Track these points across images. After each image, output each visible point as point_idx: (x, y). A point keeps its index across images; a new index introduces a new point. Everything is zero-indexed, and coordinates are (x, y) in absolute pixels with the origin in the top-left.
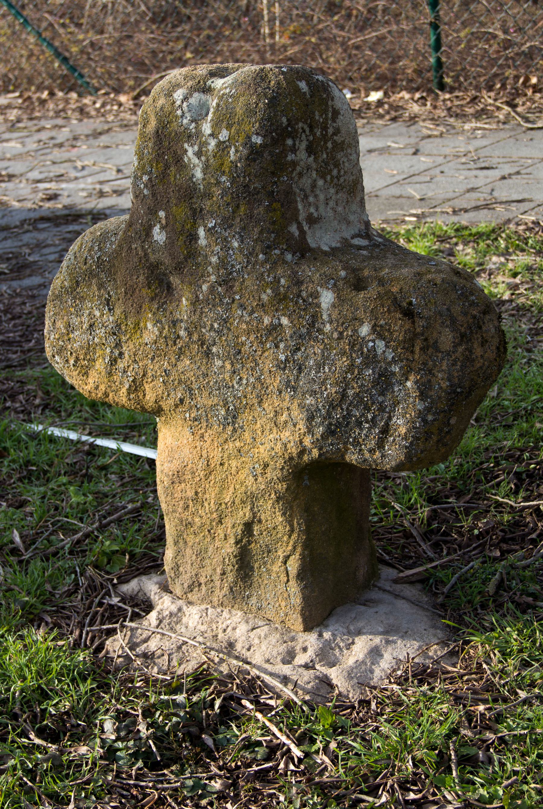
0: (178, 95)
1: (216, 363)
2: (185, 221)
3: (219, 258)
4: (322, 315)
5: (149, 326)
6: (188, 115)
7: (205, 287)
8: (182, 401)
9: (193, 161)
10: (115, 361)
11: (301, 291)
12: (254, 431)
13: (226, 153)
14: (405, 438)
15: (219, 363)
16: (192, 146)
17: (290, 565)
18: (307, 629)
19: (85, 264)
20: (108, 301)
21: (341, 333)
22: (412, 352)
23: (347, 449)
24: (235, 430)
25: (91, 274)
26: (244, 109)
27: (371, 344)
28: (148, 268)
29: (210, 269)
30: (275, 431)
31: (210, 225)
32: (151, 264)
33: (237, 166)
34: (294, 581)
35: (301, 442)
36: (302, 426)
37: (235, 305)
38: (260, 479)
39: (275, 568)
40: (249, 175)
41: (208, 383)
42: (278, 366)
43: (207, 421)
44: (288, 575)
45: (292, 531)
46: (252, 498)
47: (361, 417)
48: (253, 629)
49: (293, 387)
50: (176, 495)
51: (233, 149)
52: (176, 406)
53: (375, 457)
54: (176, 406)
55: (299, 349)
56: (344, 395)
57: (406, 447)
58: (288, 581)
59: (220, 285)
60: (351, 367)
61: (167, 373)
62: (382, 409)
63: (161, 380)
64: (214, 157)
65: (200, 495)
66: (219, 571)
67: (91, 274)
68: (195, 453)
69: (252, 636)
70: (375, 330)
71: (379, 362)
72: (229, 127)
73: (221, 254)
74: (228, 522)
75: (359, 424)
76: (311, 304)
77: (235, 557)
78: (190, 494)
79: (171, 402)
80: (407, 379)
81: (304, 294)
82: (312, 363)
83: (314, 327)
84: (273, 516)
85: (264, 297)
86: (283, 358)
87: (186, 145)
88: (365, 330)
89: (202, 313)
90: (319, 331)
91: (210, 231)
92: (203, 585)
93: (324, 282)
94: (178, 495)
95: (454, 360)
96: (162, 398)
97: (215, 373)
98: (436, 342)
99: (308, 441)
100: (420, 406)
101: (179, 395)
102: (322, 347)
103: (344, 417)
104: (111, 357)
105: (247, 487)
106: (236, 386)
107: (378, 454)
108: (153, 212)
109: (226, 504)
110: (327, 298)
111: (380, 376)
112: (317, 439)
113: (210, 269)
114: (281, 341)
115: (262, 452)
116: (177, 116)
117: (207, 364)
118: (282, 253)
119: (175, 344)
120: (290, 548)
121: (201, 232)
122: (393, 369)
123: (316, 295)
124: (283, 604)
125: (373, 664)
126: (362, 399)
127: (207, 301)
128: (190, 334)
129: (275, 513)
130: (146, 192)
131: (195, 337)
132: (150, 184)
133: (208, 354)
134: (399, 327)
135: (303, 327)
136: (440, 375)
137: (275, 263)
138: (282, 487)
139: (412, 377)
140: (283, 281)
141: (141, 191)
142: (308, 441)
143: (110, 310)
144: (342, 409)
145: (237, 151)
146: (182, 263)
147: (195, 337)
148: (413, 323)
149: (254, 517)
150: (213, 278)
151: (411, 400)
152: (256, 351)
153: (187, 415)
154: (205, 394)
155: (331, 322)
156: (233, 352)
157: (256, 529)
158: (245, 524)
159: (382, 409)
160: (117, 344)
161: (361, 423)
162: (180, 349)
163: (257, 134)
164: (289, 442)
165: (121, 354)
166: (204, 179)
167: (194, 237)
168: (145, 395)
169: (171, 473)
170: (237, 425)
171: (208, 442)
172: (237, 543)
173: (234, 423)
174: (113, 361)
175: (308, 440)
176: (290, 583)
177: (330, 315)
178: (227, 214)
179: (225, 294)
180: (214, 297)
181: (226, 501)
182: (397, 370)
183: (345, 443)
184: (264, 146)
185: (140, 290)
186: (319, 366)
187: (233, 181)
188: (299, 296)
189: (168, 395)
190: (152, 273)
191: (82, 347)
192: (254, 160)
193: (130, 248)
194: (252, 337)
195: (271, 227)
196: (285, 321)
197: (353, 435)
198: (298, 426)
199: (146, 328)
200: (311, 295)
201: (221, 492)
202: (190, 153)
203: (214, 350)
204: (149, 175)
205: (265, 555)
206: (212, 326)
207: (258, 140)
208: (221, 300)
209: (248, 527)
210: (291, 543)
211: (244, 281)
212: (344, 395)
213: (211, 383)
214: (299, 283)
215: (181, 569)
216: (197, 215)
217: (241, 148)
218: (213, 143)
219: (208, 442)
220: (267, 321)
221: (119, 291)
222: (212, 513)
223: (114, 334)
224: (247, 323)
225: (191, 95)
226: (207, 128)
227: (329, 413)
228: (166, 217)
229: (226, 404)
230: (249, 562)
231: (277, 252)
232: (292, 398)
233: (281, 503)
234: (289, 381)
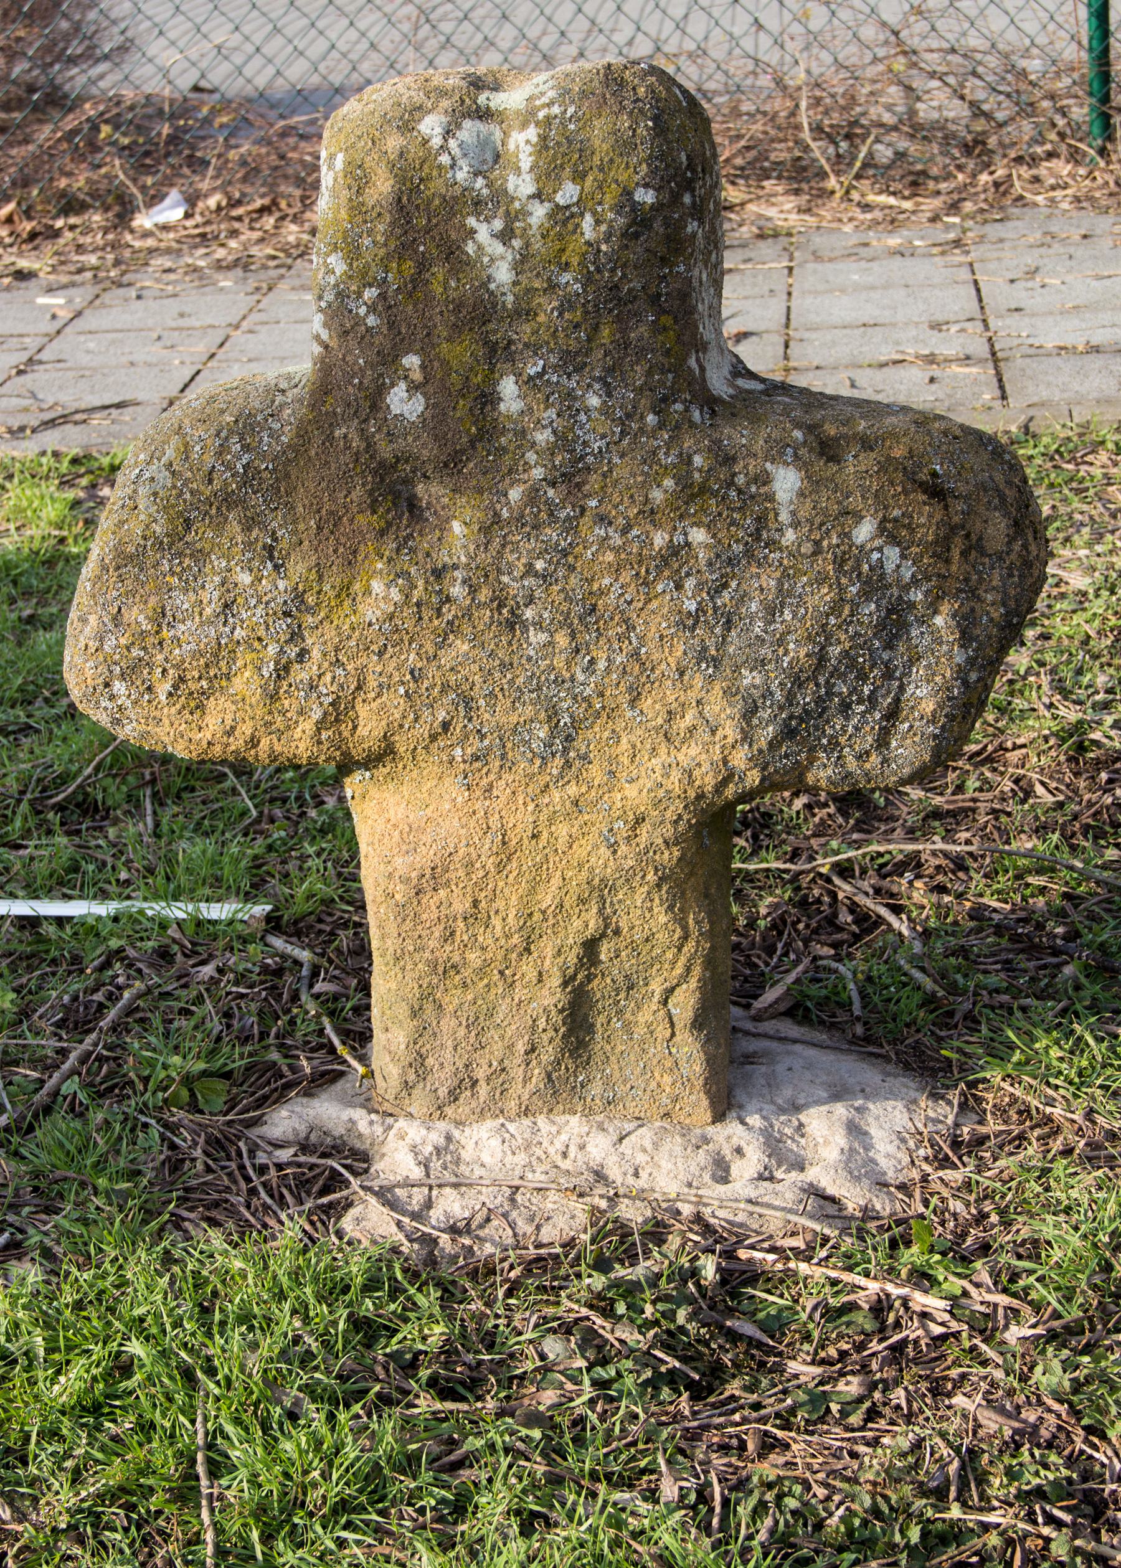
0: (431, 126)
1: (532, 639)
2: (471, 369)
3: (554, 432)
4: (777, 515)
5: (377, 586)
6: (462, 162)
7: (515, 494)
8: (446, 726)
9: (489, 250)
10: (286, 669)
11: (734, 475)
12: (613, 759)
13: (570, 227)
14: (933, 721)
15: (537, 638)
16: (487, 220)
17: (675, 1006)
18: (719, 1117)
19: (210, 481)
20: (270, 549)
21: (817, 543)
22: (948, 561)
23: (811, 760)
24: (568, 764)
25: (228, 500)
26: (612, 141)
27: (876, 556)
28: (375, 472)
29: (531, 457)
30: (663, 750)
31: (532, 371)
32: (382, 464)
33: (599, 251)
34: (687, 1034)
35: (725, 762)
36: (730, 731)
37: (587, 520)
38: (623, 849)
39: (644, 1016)
40: (624, 266)
41: (512, 682)
42: (681, 624)
43: (503, 757)
44: (672, 1025)
45: (685, 938)
46: (601, 891)
47: (850, 694)
48: (621, 1139)
49: (714, 659)
50: (424, 917)
51: (588, 219)
52: (433, 738)
53: (868, 766)
54: (433, 738)
55: (725, 586)
56: (822, 658)
57: (935, 737)
58: (673, 1035)
59: (553, 484)
60: (835, 608)
61: (416, 676)
62: (888, 675)
63: (402, 691)
64: (543, 237)
65: (483, 904)
66: (521, 1047)
67: (228, 500)
68: (472, 823)
69: (628, 1152)
70: (884, 529)
71: (888, 587)
72: (579, 177)
73: (559, 424)
74: (547, 947)
75: (845, 708)
77: (561, 1011)
78: (461, 906)
79: (422, 730)
80: (936, 612)
81: (741, 480)
82: (754, 607)
83: (758, 539)
84: (647, 916)
85: (657, 495)
86: (693, 607)
87: (471, 221)
88: (864, 532)
89: (503, 546)
90: (772, 544)
91: (530, 383)
92: (482, 1083)
93: (777, 451)
94: (429, 915)
95: (1010, 568)
96: (401, 726)
97: (529, 659)
98: (980, 539)
99: (739, 759)
100: (959, 658)
101: (442, 715)
102: (778, 574)
103: (819, 700)
104: (277, 663)
105: (592, 870)
106: (580, 677)
107: (875, 759)
108: (388, 359)
109: (544, 912)
110: (786, 482)
111: (890, 612)
112: (760, 751)
113: (531, 457)
114: (688, 575)
115: (632, 795)
116: (440, 167)
117: (510, 644)
118: (687, 410)
119: (439, 613)
120: (679, 970)
121: (508, 387)
122: (912, 597)
123: (764, 479)
124: (667, 1079)
125: (867, 1149)
126: (855, 660)
127: (519, 520)
128: (473, 590)
129: (650, 910)
130: (371, 321)
131: (484, 595)
132: (384, 305)
133: (514, 623)
134: (926, 518)
135: (737, 541)
136: (989, 597)
137: (677, 427)
138: (669, 857)
139: (945, 607)
140: (698, 460)
141: (359, 321)
142: (739, 759)
143: (276, 567)
144: (817, 685)
145: (598, 222)
146: (463, 452)
147: (484, 595)
148: (946, 507)
149: (606, 927)
150: (538, 473)
151: (945, 648)
152: (630, 603)
153: (458, 752)
154: (503, 703)
155: (796, 525)
156: (578, 609)
157: (605, 951)
158: (584, 944)
159: (888, 675)
160: (293, 634)
161: (848, 706)
162: (450, 623)
163: (646, 186)
164: (699, 765)
165: (302, 655)
166: (515, 283)
167: (488, 398)
168: (355, 728)
169: (414, 875)
170: (572, 754)
171: (503, 799)
172: (565, 984)
173: (565, 750)
174: (283, 670)
175: (741, 755)
176: (678, 1038)
177: (793, 513)
178: (573, 345)
179: (563, 501)
180: (536, 513)
181: (544, 906)
182: (920, 596)
183: (812, 750)
184: (657, 208)
185: (352, 521)
186: (771, 612)
187: (588, 280)
188: (730, 484)
189: (416, 720)
190: (382, 480)
191: (197, 654)
192: (636, 236)
193: (330, 438)
194: (626, 576)
195: (665, 361)
196: (698, 536)
197: (829, 731)
198: (720, 733)
199: (368, 592)
200: (755, 480)
201: (532, 891)
202: (483, 233)
203: (529, 614)
204: (379, 286)
205: (622, 995)
206: (530, 566)
207: (646, 197)
208: (551, 514)
209: (591, 947)
210: (683, 960)
211: (610, 471)
212: (822, 658)
213: (520, 680)
214: (729, 460)
215: (430, 1061)
216: (498, 354)
217: (610, 215)
218: (539, 212)
219: (503, 799)
220: (660, 539)
221: (301, 527)
222: (508, 937)
223: (287, 614)
224: (617, 550)
225: (459, 126)
226: (521, 185)
227: (790, 698)
228: (423, 367)
229: (553, 715)
230: (586, 1016)
231: (679, 407)
232: (710, 680)
233: (665, 888)
234: (705, 649)
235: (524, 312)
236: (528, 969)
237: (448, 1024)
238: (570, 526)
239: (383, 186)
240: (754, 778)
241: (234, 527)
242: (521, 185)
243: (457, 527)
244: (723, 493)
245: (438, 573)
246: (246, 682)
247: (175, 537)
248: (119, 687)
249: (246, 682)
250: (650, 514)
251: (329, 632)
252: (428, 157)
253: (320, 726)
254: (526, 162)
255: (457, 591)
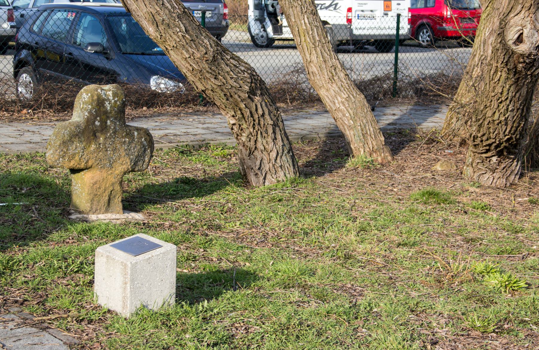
7: (109, 134)
15: (109, 152)
36: (129, 164)
39: (116, 201)
67: (77, 135)
74: (107, 192)
76: (133, 135)
78: (98, 187)
88: (143, 139)
91: (111, 121)
99: (129, 167)
108: (96, 118)
110: (136, 133)
115: (117, 172)
121: (109, 122)
123: (134, 133)
132: (95, 111)
133: (107, 150)
167: (106, 123)
186: (134, 149)
216: (108, 118)
218: (113, 101)
226: (111, 98)
235: (111, 113)
236: (104, 194)
237: (95, 202)
238: (114, 138)
239: (95, 97)
240: (131, 170)
241: (77, 138)
242: (111, 98)
243: (101, 138)
244: (129, 134)
245: (100, 144)
246: (77, 158)
247: (70, 140)
248: (61, 159)
249: (77, 158)
250: (123, 137)
251: (87, 152)
252: (100, 94)
253: (85, 163)
254: (111, 95)
255: (101, 146)
